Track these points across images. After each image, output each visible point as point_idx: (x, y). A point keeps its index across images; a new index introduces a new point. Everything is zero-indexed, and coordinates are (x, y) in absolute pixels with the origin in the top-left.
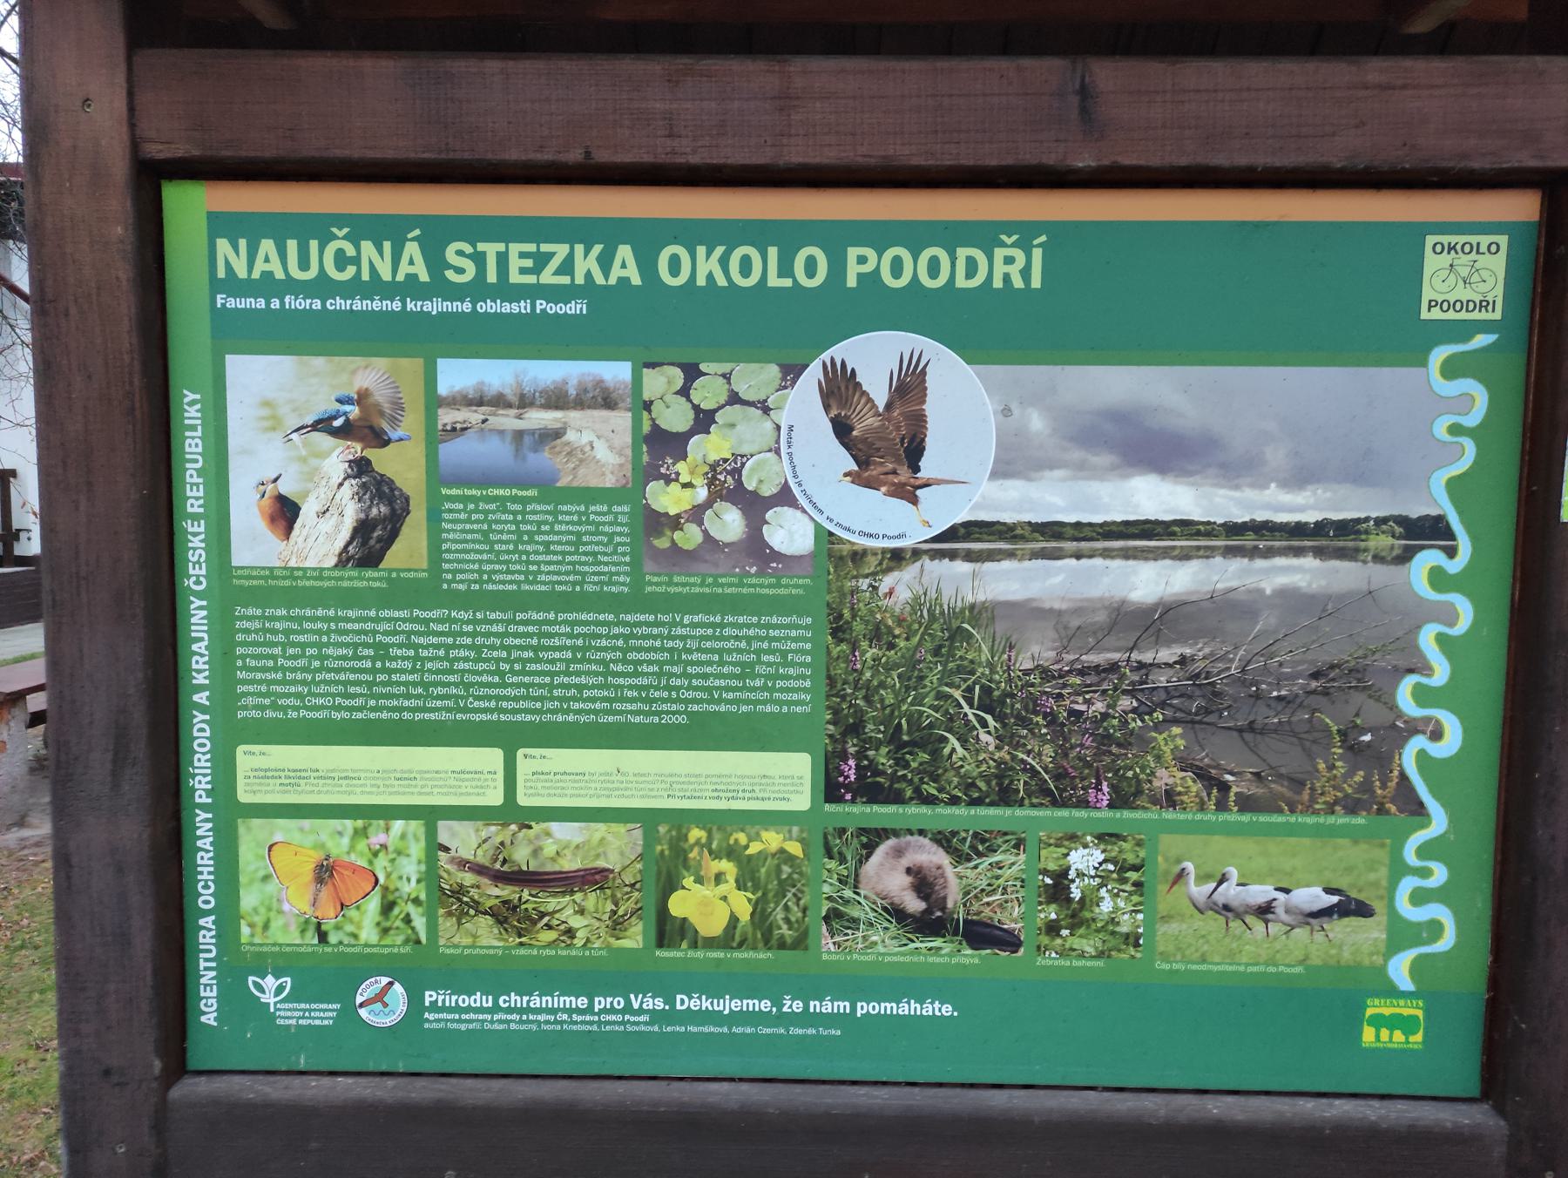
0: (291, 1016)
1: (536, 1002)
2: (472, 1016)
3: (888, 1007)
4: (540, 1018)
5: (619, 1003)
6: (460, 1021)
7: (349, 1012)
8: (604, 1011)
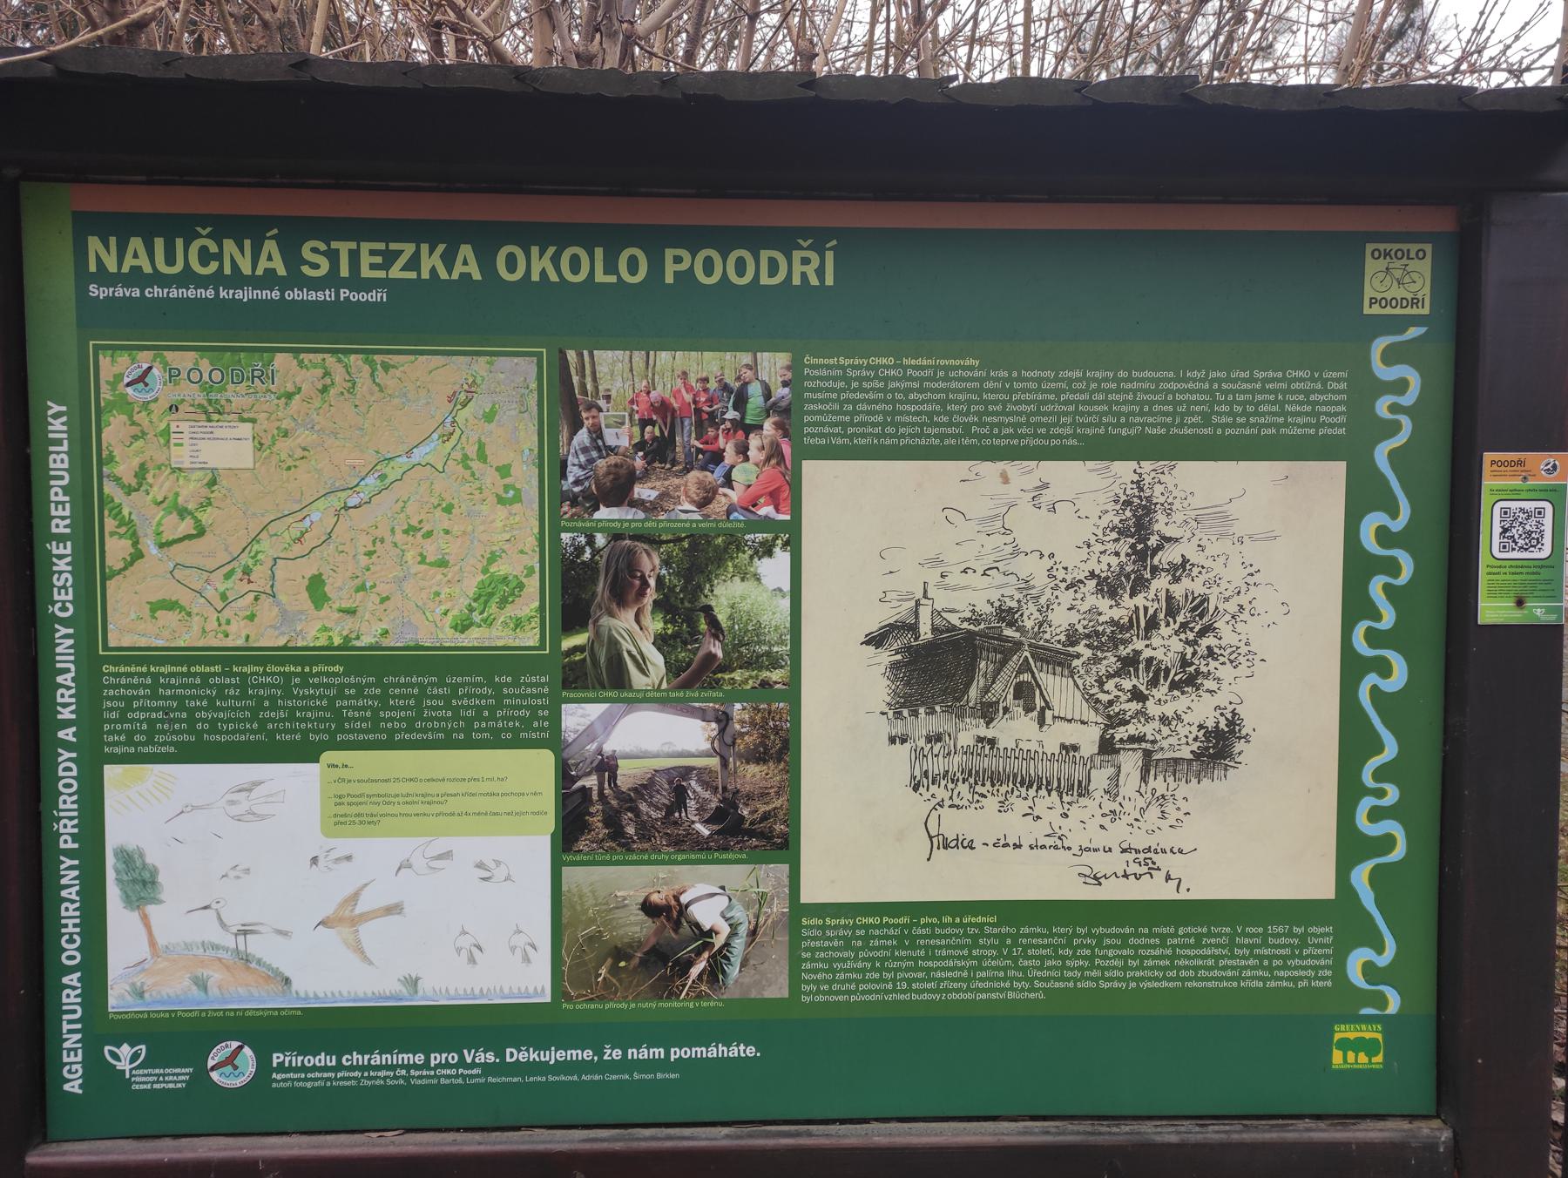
0: (144, 1081)
1: (377, 1059)
2: (318, 1075)
3: (699, 1051)
4: (382, 1074)
5: (453, 1058)
6: (306, 1080)
7: (201, 1075)
8: (439, 1066)
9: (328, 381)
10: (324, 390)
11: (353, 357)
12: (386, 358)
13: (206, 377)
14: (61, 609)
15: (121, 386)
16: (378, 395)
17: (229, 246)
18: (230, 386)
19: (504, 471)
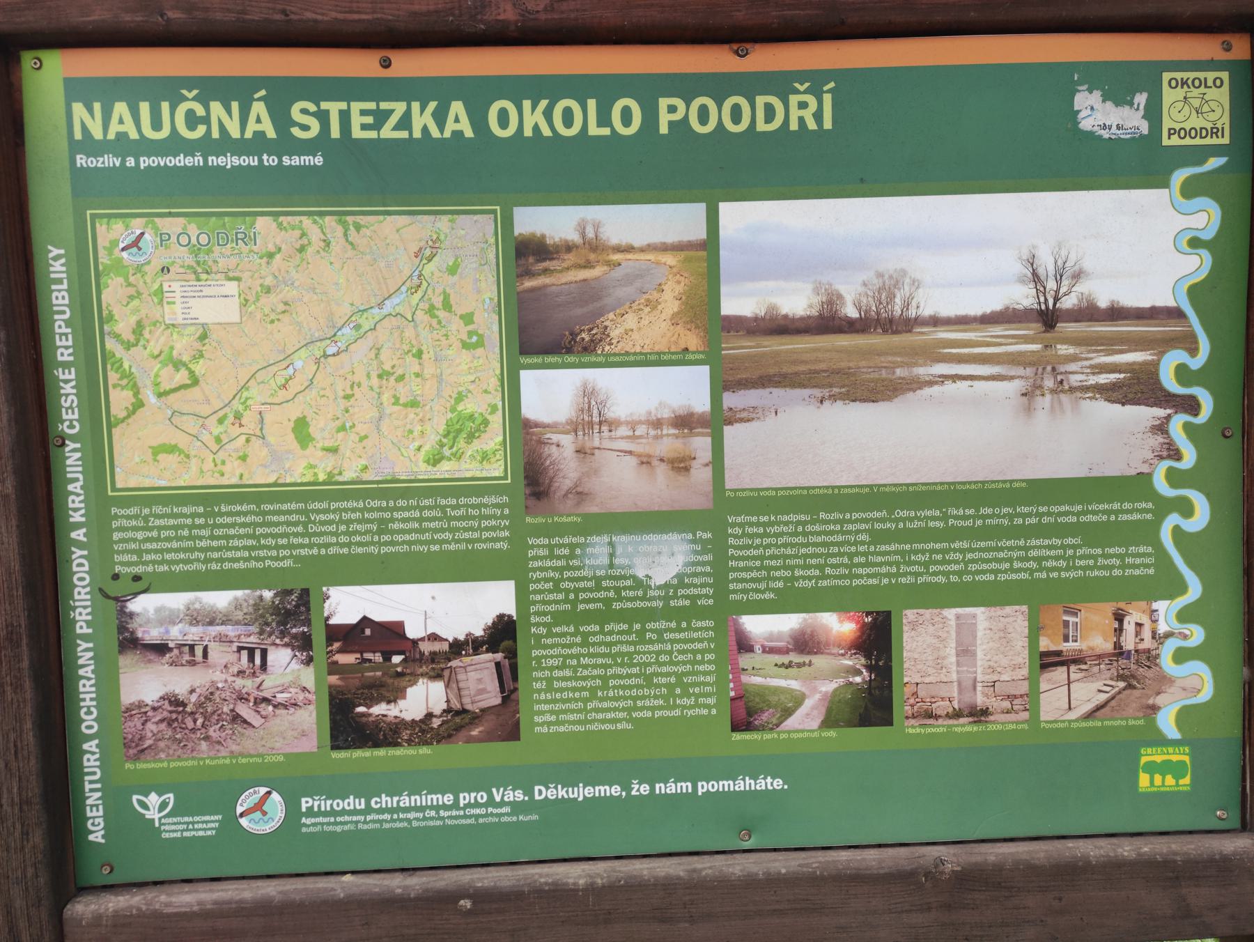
0: (173, 829)
1: (406, 801)
2: (347, 818)
3: (725, 785)
4: (411, 815)
5: (482, 797)
6: (336, 823)
7: (231, 821)
8: (469, 805)
9: (305, 241)
10: (302, 249)
11: (327, 219)
12: (358, 219)
13: (194, 240)
14: (69, 427)
15: (116, 251)
16: (350, 253)
17: (216, 108)
18: (217, 249)
19: (468, 318)
